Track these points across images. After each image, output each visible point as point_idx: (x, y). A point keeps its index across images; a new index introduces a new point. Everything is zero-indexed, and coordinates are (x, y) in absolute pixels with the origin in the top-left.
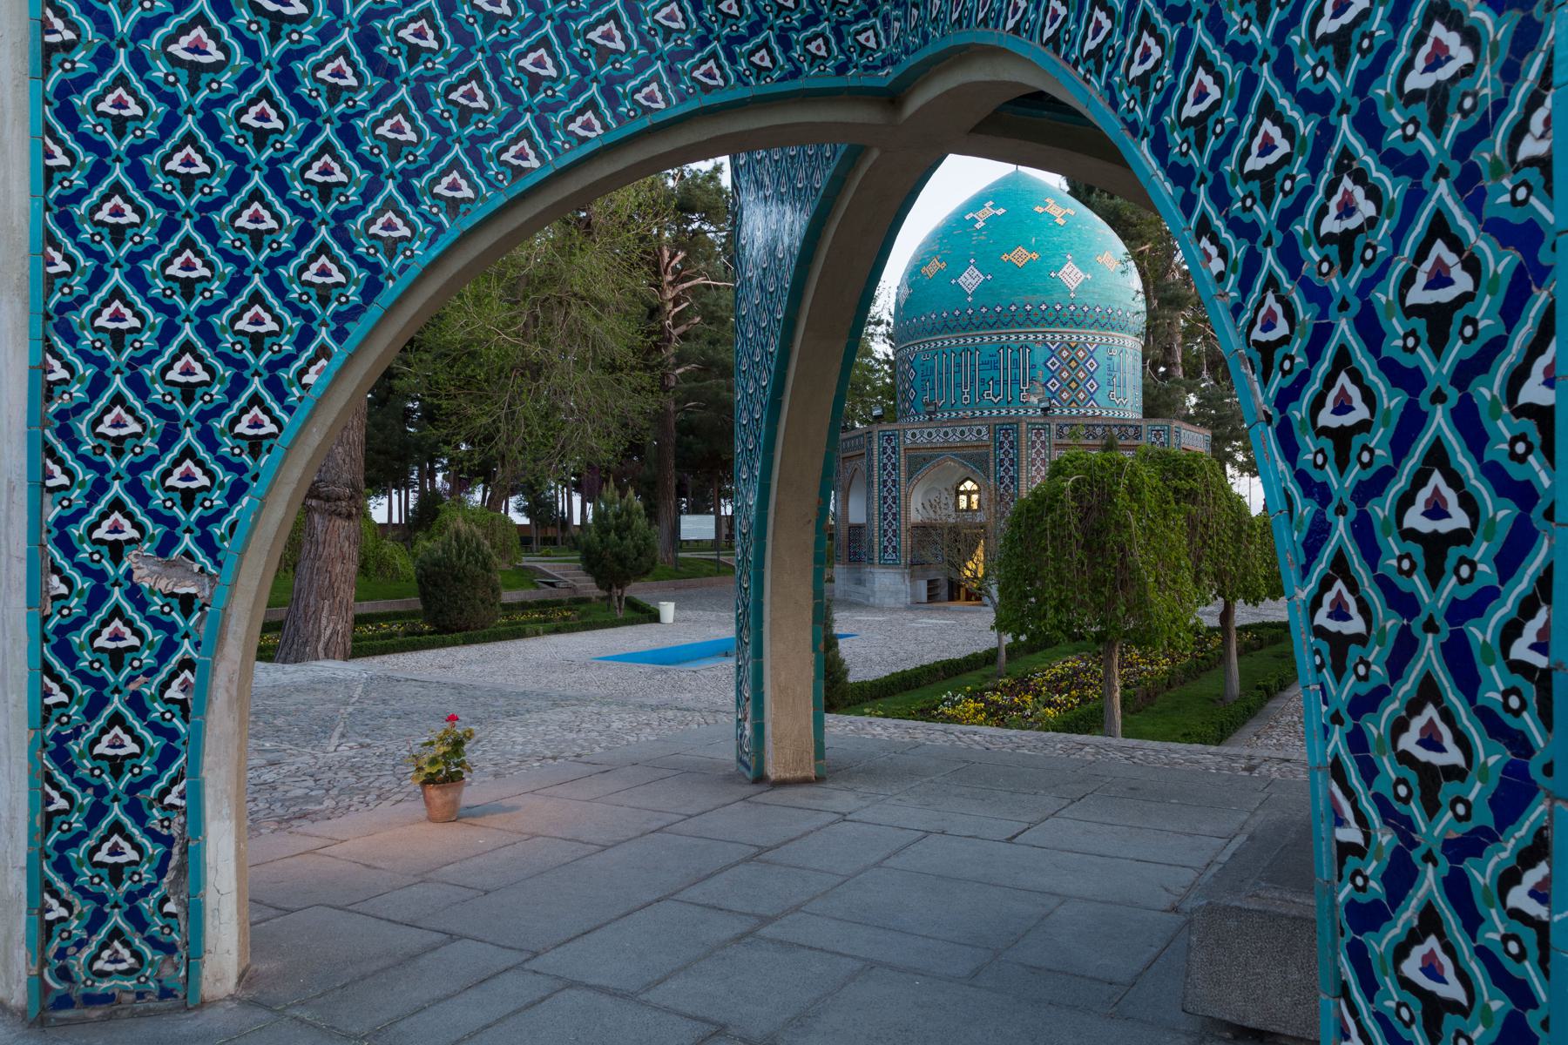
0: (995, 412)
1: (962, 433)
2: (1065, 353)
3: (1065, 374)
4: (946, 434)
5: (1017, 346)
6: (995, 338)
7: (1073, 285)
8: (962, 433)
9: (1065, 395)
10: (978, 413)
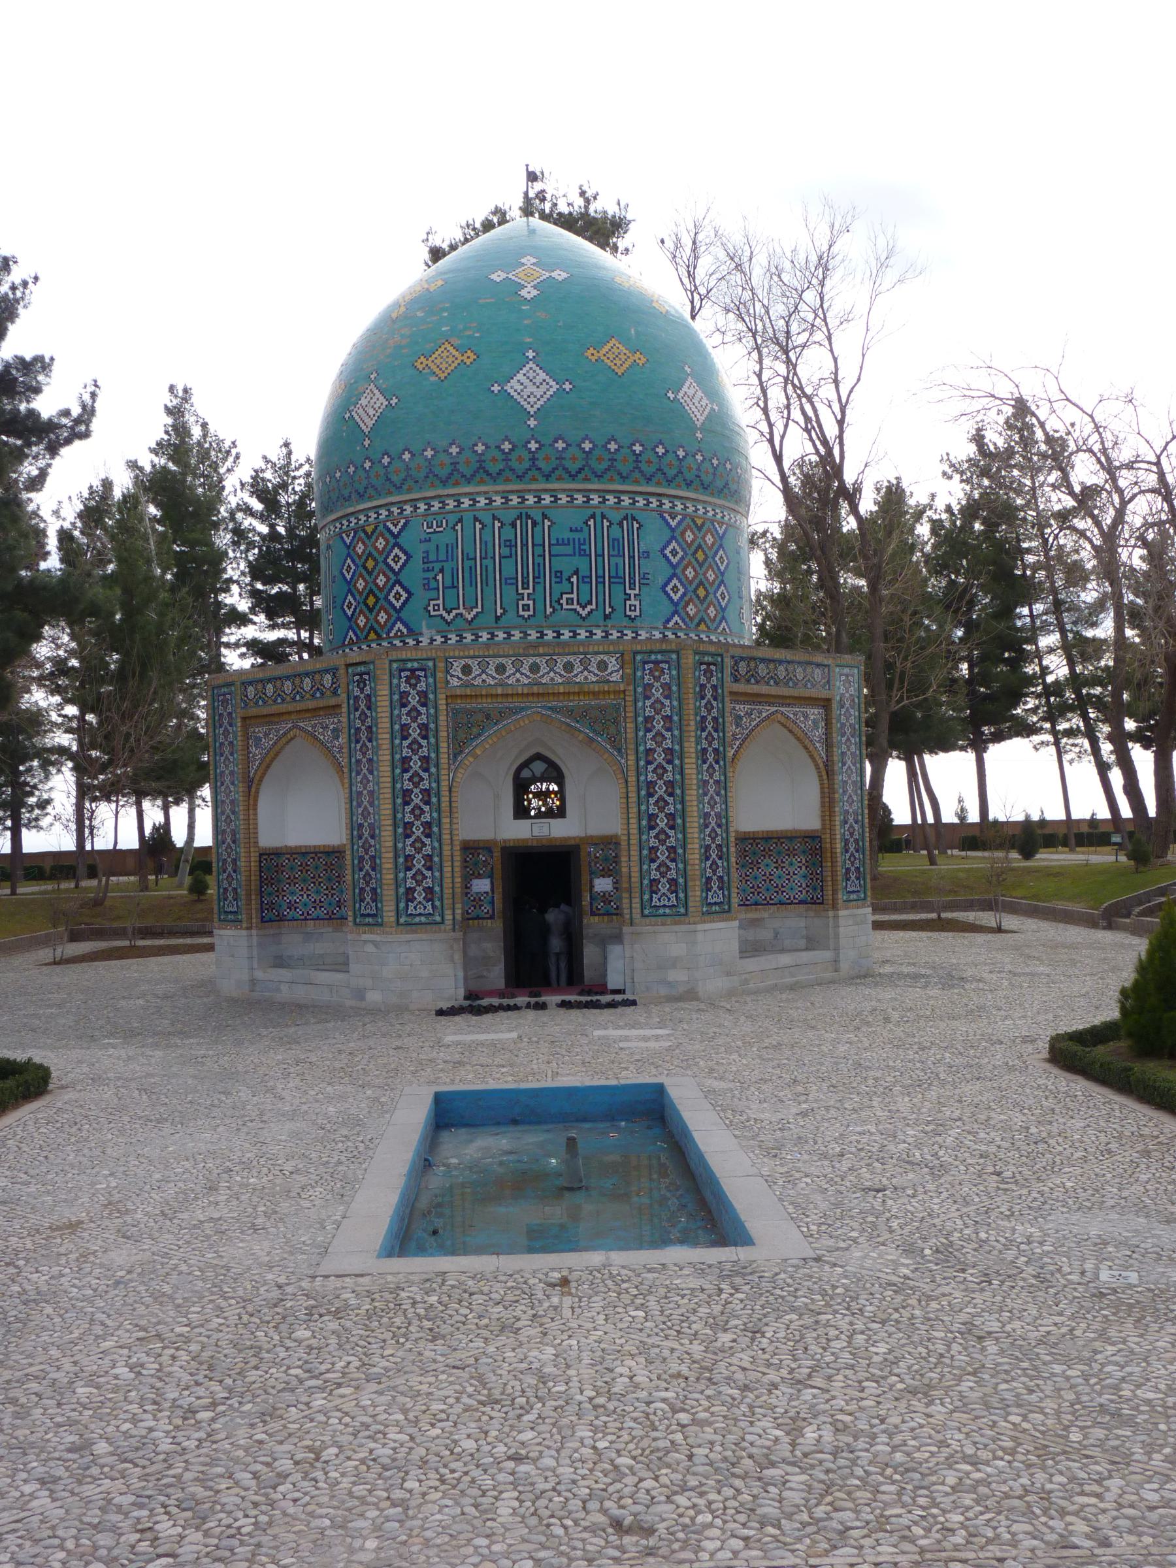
0: (583, 634)
1: (568, 667)
2: (689, 536)
3: (690, 573)
4: (535, 668)
5: (616, 516)
6: (580, 499)
7: (700, 418)
8: (568, 667)
9: (691, 610)
10: (550, 635)
